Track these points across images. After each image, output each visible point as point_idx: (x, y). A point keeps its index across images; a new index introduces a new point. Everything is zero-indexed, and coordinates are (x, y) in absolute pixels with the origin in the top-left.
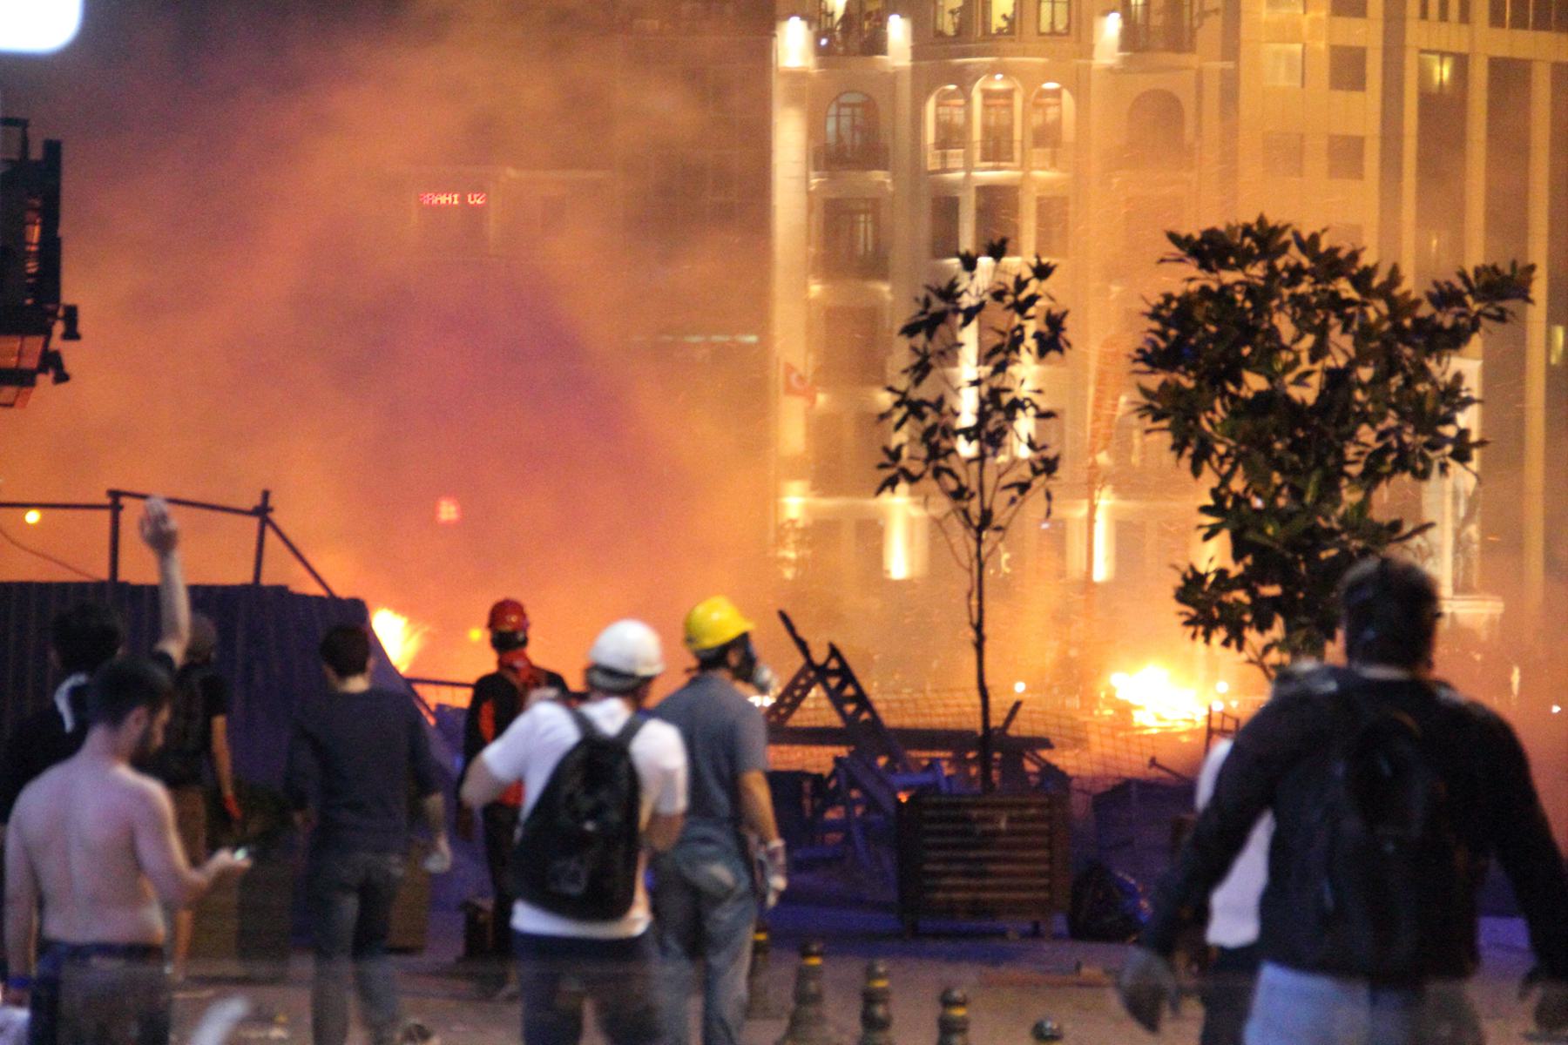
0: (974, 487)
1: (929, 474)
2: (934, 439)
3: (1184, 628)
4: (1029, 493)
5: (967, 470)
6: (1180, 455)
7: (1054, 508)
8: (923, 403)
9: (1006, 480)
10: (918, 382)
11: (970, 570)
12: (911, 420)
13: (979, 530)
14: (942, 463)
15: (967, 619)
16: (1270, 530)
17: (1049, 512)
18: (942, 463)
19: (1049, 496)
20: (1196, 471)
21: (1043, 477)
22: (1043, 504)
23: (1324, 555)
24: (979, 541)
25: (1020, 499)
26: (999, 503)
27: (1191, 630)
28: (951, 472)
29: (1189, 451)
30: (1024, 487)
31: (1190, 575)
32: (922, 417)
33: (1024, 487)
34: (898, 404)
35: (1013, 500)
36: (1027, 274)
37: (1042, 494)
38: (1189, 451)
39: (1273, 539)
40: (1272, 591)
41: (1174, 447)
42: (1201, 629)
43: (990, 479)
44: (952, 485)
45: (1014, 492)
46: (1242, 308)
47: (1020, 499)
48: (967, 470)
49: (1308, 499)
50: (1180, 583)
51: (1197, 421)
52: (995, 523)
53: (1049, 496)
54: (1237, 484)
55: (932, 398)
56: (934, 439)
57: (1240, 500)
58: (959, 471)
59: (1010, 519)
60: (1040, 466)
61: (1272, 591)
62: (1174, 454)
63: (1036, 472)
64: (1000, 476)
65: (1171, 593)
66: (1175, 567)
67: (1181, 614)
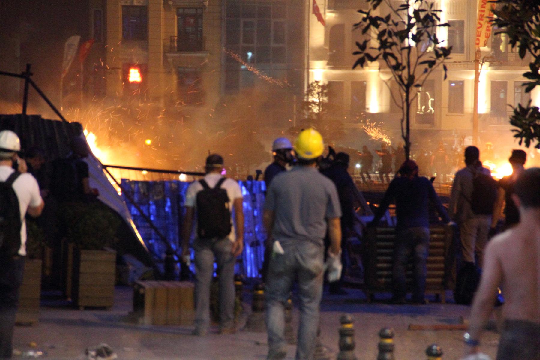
0: (405, 63)
1: (381, 57)
2: (384, 38)
3: (515, 138)
4: (434, 67)
5: (401, 54)
6: (513, 46)
7: (448, 75)
8: (378, 18)
9: (421, 60)
10: (375, 7)
11: (403, 109)
12: (372, 28)
13: (408, 87)
14: (388, 50)
15: (401, 134)
17: (446, 77)
18: (388, 50)
19: (445, 68)
20: (522, 54)
21: (442, 59)
22: (444, 72)
24: (408, 92)
25: (429, 70)
26: (419, 72)
27: (519, 139)
28: (392, 55)
29: (518, 43)
30: (432, 64)
31: (518, 110)
32: (377, 26)
33: (432, 64)
34: (365, 20)
35: (426, 71)
37: (441, 67)
38: (518, 43)
41: (511, 42)
42: (524, 139)
43: (413, 60)
44: (393, 62)
45: (426, 66)
47: (429, 70)
48: (401, 54)
50: (512, 114)
51: (523, 27)
52: (417, 82)
53: (445, 68)
55: (384, 16)
56: (384, 38)
58: (398, 55)
59: (424, 81)
60: (441, 52)
62: (510, 46)
63: (438, 56)
64: (419, 58)
65: (508, 119)
66: (511, 106)
67: (513, 131)
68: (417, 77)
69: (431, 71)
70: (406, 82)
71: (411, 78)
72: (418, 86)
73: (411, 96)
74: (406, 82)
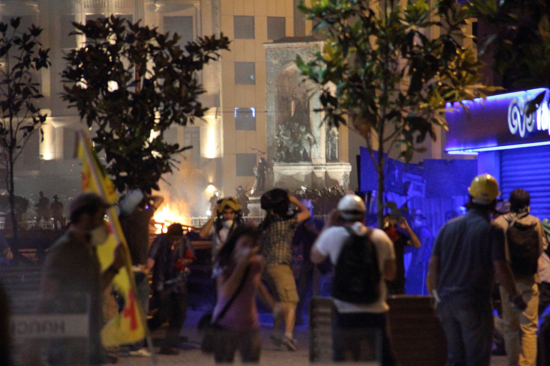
9: (21, 126)
16: (121, 149)
23: (144, 158)
24: (11, 153)
35: (25, 134)
36: (29, 33)
39: (122, 152)
40: (124, 174)
45: (26, 130)
46: (106, 54)
47: (28, 134)
49: (136, 135)
52: (18, 144)
54: (108, 129)
57: (110, 135)
61: (124, 174)
64: (19, 124)
68: (18, 140)
69: (30, 135)
70: (9, 145)
71: (14, 141)
72: (19, 147)
73: (14, 156)
74: (9, 145)
